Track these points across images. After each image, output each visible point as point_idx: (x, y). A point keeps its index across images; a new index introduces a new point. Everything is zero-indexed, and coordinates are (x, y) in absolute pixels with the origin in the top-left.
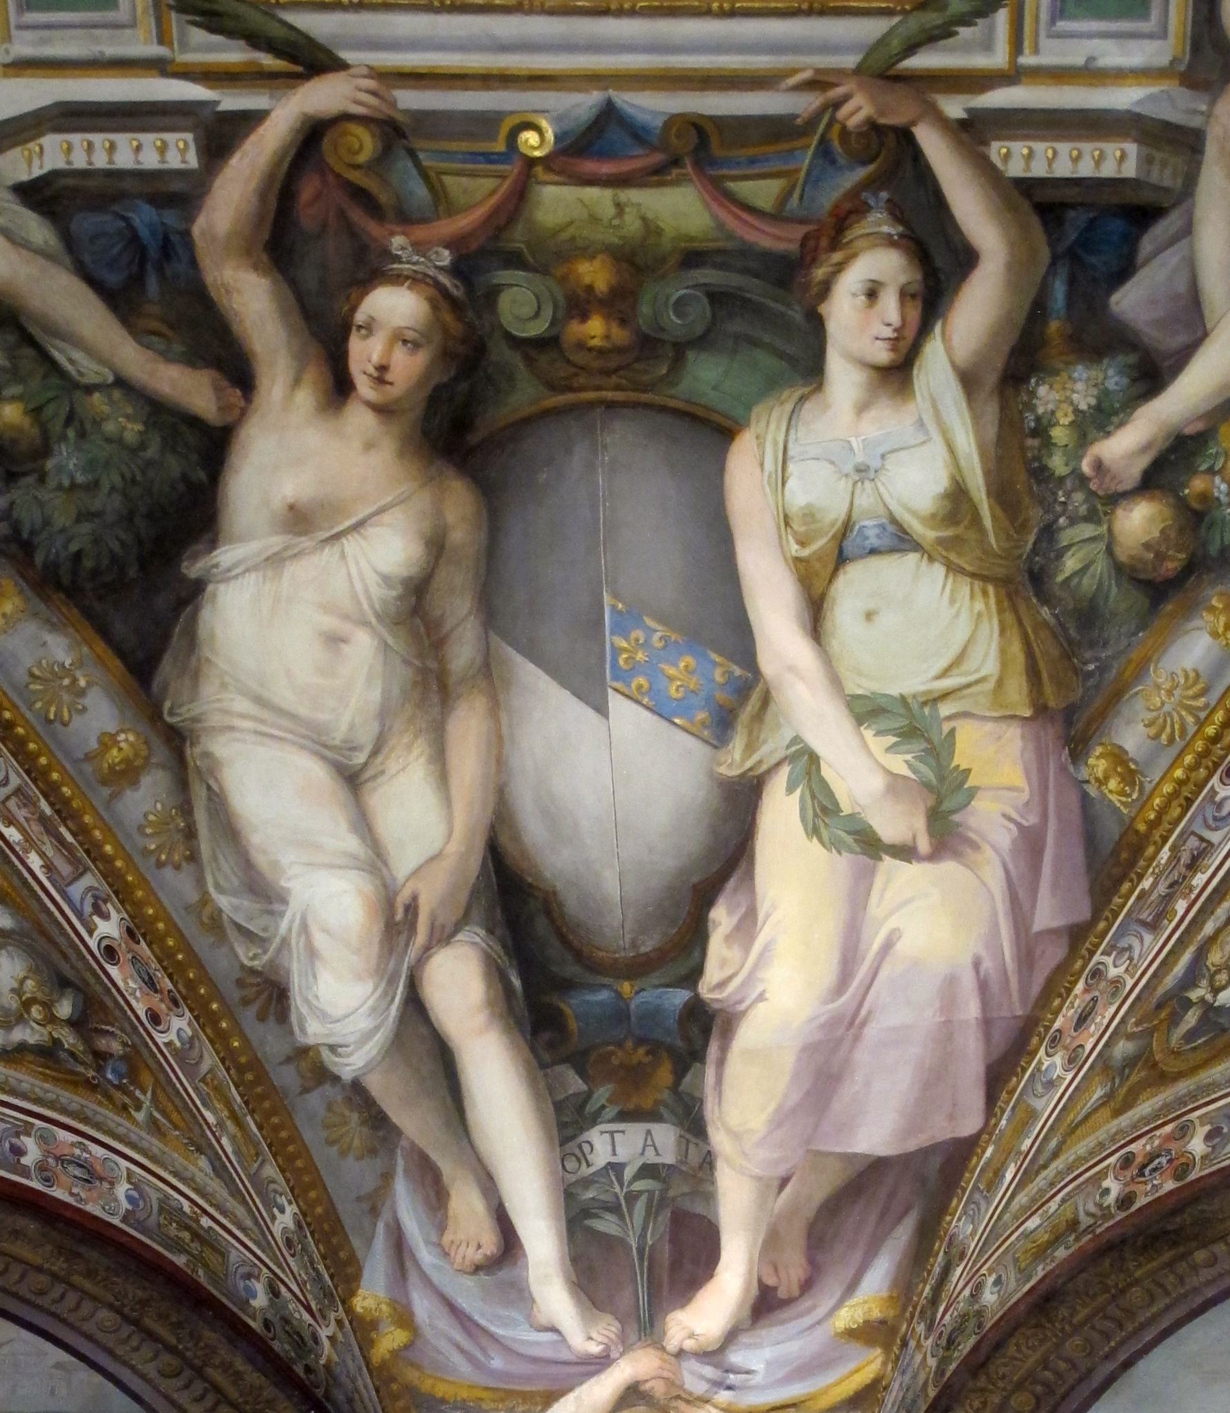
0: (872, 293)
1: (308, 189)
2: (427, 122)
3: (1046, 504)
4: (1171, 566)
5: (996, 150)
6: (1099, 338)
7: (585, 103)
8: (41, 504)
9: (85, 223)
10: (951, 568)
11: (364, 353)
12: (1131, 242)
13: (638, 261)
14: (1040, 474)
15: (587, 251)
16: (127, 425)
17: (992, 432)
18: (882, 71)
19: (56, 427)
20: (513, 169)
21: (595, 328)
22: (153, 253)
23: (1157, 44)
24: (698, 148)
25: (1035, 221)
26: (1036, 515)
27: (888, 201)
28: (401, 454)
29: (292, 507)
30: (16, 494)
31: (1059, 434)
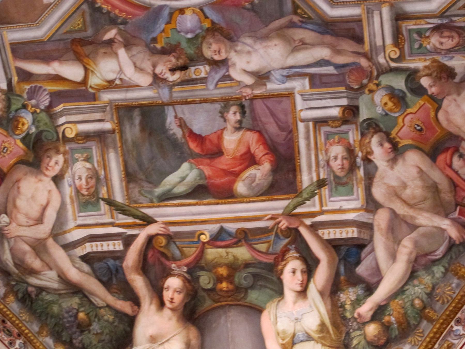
0: (294, 272)
1: (150, 254)
2: (177, 234)
3: (346, 325)
4: (382, 341)
5: (320, 232)
6: (355, 281)
7: (215, 227)
8: (90, 338)
9: (97, 265)
10: (323, 345)
11: (167, 295)
12: (359, 254)
13: (234, 267)
14: (344, 318)
15: (220, 265)
16: (110, 317)
17: (329, 307)
18: (289, 214)
19: (92, 318)
20: (200, 245)
21: (224, 285)
22: (114, 272)
23: (357, 201)
24: (244, 237)
25: (333, 250)
26: (344, 329)
27: (295, 247)
28: (178, 321)
29: (151, 336)
30: (83, 336)
31: (348, 307)
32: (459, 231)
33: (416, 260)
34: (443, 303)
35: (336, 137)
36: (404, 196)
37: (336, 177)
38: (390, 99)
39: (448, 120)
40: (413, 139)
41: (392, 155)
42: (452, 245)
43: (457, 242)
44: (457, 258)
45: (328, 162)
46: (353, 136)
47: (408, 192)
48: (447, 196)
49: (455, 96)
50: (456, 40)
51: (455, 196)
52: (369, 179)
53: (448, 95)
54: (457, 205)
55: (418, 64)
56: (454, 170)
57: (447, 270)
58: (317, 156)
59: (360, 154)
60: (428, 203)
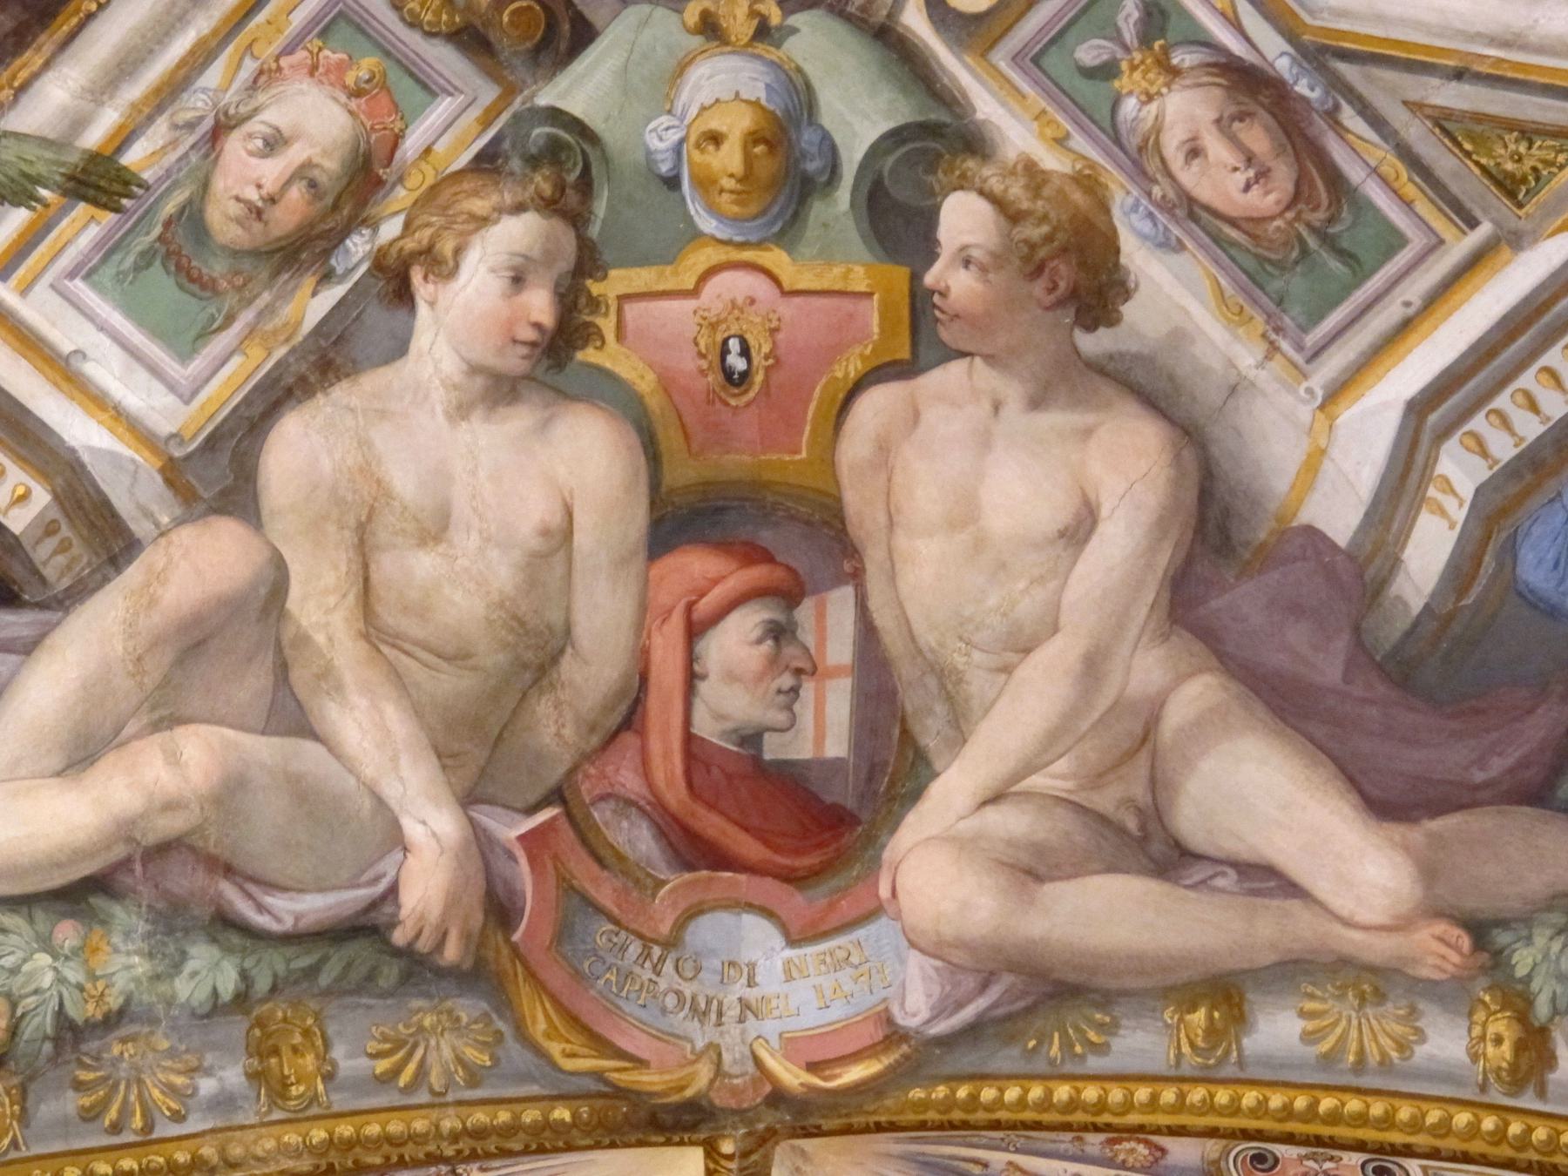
23: (171, 400)
32: (452, 901)
33: (165, 848)
34: (90, 1115)
35: (368, 64)
36: (386, 567)
37: (192, 218)
38: (753, 138)
39: (884, 450)
40: (666, 383)
41: (514, 361)
42: (366, 928)
43: (399, 937)
44: (327, 993)
45: (220, 129)
46: (446, 123)
47: (424, 564)
48: (553, 731)
49: (1014, 392)
50: (1263, 201)
51: (587, 757)
52: (326, 361)
53: (990, 359)
54: (557, 796)
55: (1016, 124)
56: (691, 658)
57: (242, 1000)
58: (201, 57)
59: (390, 229)
60: (448, 684)
